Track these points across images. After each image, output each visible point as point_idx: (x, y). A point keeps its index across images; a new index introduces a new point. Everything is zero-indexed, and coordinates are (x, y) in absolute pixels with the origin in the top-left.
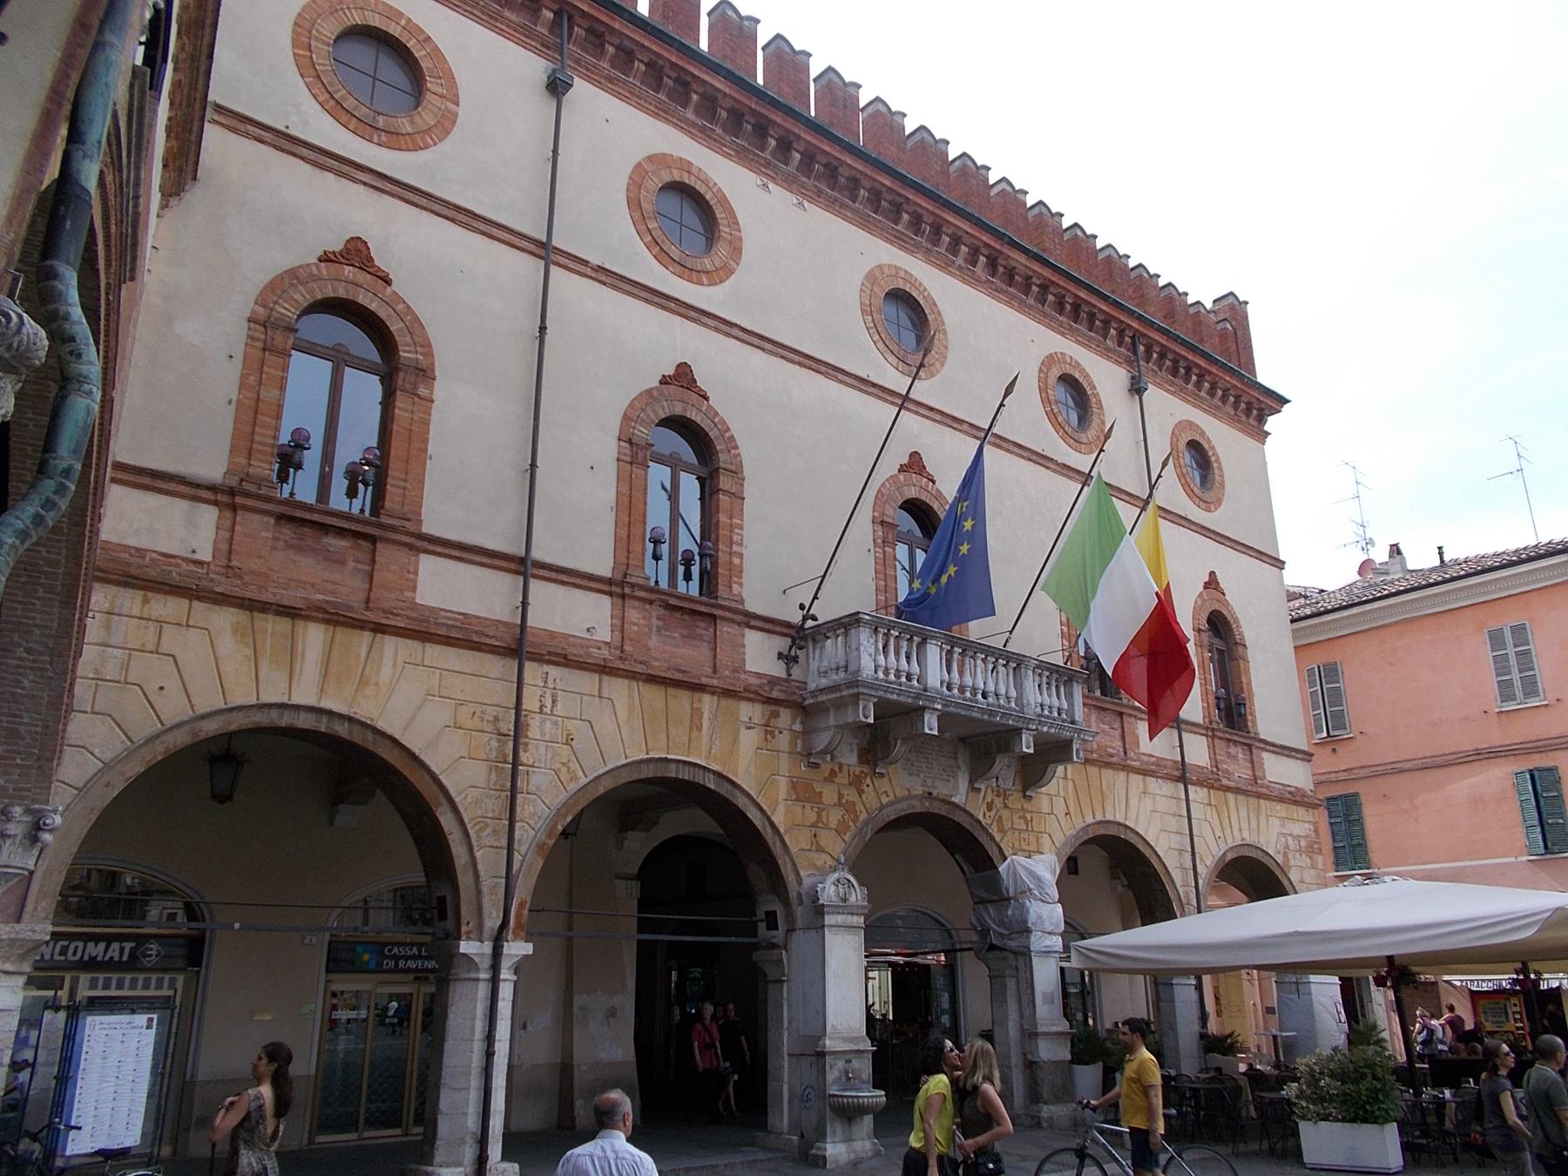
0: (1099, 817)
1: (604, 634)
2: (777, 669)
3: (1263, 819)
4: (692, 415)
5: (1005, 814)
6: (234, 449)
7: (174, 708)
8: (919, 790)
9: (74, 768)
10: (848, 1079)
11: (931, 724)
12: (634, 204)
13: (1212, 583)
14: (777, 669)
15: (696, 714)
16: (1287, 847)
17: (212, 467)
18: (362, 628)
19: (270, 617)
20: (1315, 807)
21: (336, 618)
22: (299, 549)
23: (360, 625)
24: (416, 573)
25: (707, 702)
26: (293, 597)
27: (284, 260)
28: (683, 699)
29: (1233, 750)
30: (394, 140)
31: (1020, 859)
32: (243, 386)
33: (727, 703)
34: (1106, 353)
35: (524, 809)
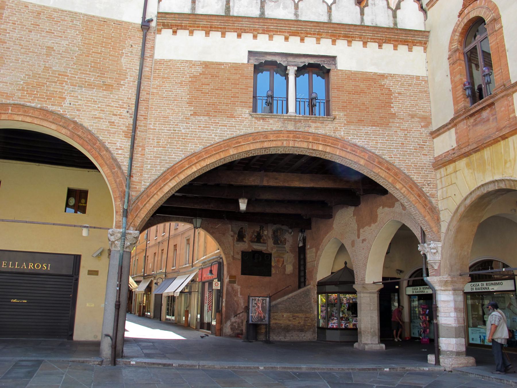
6: (454, 105)
7: (459, 199)
9: (444, 229)
17: (450, 115)
18: (499, 141)
19: (474, 155)
22: (476, 125)
23: (496, 141)
24: (513, 104)
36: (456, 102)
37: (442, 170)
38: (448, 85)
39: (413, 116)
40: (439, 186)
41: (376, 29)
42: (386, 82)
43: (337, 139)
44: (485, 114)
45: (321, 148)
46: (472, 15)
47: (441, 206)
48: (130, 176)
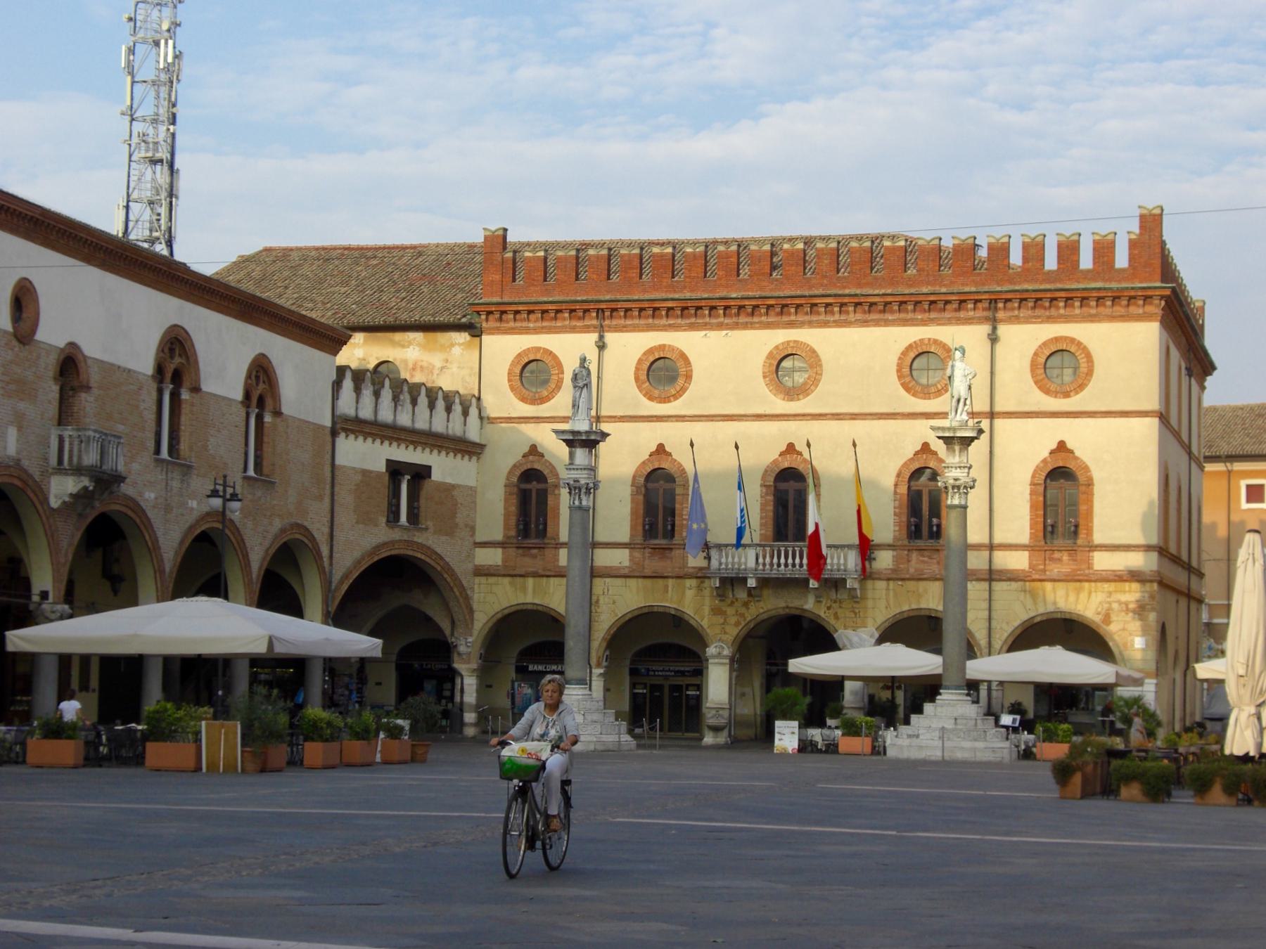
0: (914, 606)
1: (627, 563)
2: (704, 563)
3: (1083, 596)
5: (840, 611)
7: (497, 608)
8: (783, 605)
10: (718, 716)
11: (752, 583)
12: (637, 379)
13: (1062, 446)
14: (704, 563)
15: (666, 587)
16: (1110, 609)
17: (498, 536)
20: (1151, 581)
21: (535, 575)
25: (670, 582)
26: (522, 571)
28: (660, 581)
29: (1057, 555)
30: (542, 400)
31: (850, 632)
32: (505, 509)
33: (679, 581)
34: (968, 321)
35: (595, 626)
36: (506, 527)
37: (483, 580)
38: (499, 508)
39: (466, 526)
40: (476, 590)
42: (455, 493)
43: (429, 548)
44: (534, 551)
45: (419, 555)
46: (536, 466)
47: (475, 606)
48: (330, 582)
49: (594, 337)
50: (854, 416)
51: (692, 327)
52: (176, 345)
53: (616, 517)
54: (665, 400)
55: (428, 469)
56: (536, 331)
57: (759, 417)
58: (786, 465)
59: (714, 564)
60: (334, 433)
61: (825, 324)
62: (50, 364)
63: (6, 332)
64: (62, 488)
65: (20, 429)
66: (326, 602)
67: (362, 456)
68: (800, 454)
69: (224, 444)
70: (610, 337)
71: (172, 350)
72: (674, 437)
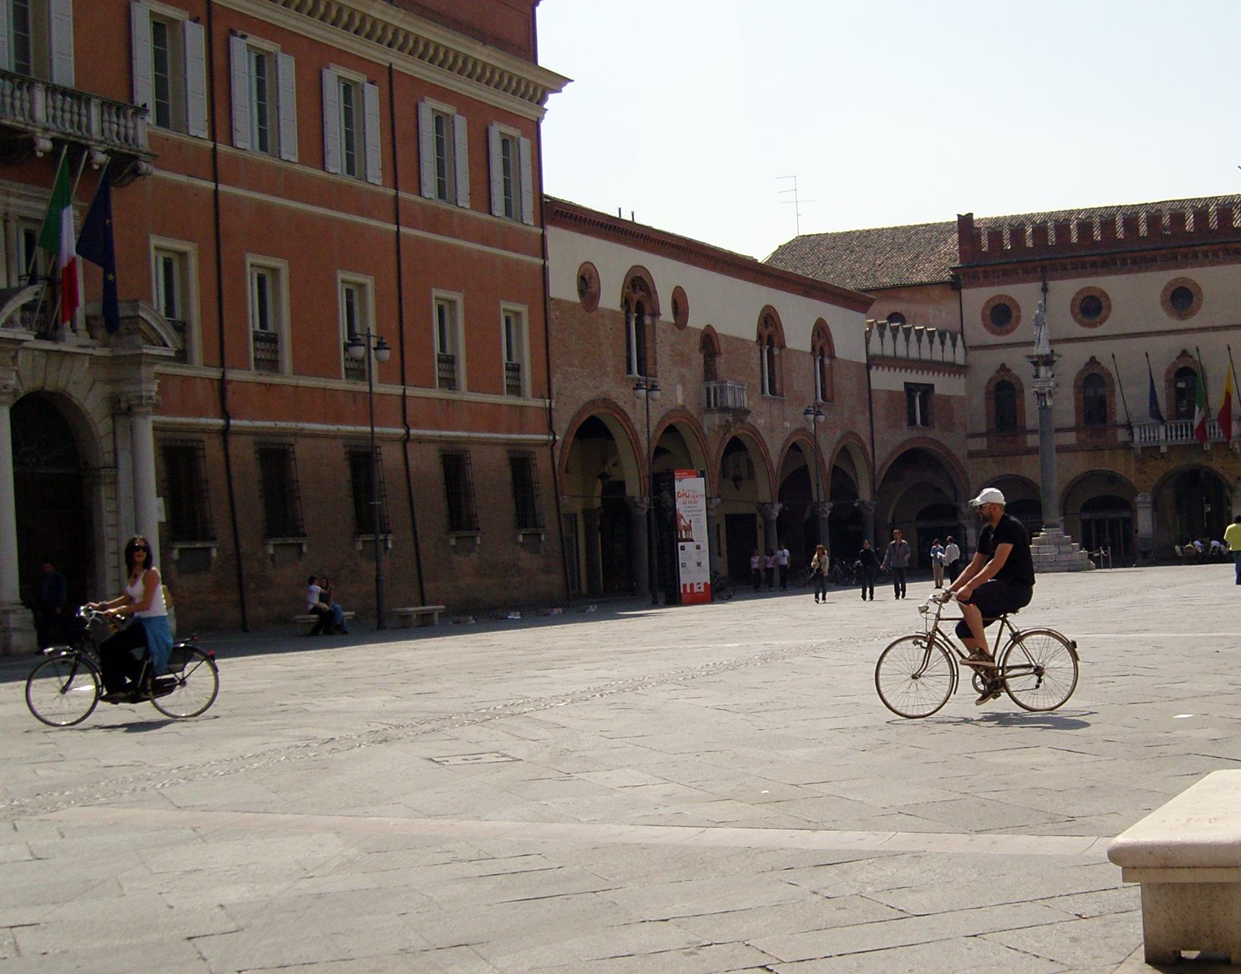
1: (1074, 441)
2: (1127, 438)
4: (1096, 371)
11: (1163, 449)
12: (1072, 312)
17: (983, 429)
27: (988, 377)
30: (1008, 332)
41: (948, 364)
43: (937, 442)
49: (1041, 284)
50: (1227, 328)
51: (1110, 273)
52: (769, 319)
53: (1065, 408)
54: (1094, 326)
55: (932, 386)
56: (1000, 284)
57: (1159, 333)
58: (1181, 365)
59: (1136, 437)
60: (868, 367)
61: (1202, 266)
62: (696, 340)
63: (670, 323)
64: (712, 422)
65: (684, 385)
66: (873, 483)
67: (887, 381)
68: (1191, 357)
69: (802, 380)
70: (1051, 284)
71: (766, 322)
72: (1102, 351)
